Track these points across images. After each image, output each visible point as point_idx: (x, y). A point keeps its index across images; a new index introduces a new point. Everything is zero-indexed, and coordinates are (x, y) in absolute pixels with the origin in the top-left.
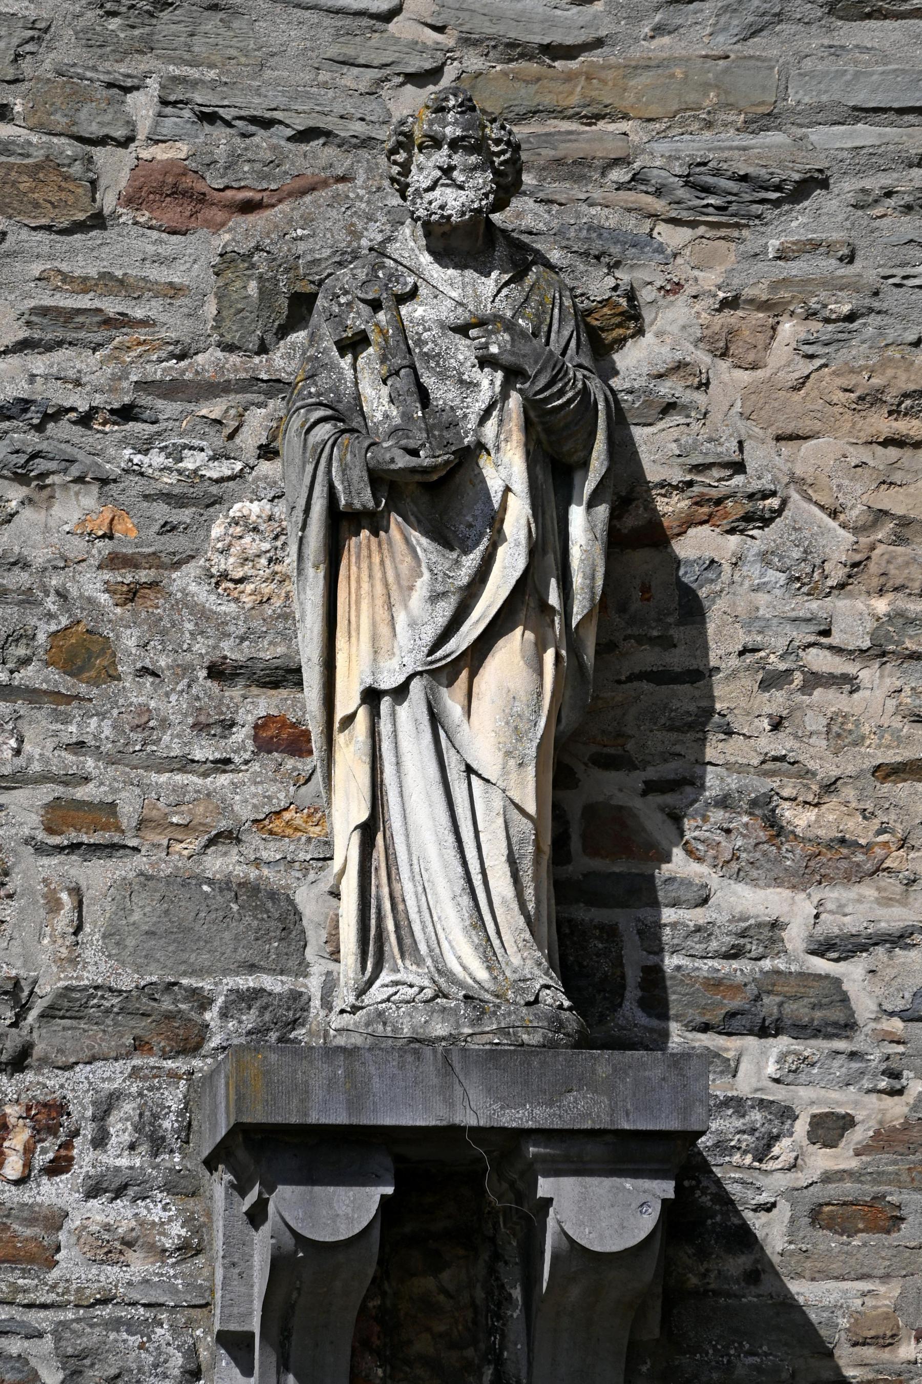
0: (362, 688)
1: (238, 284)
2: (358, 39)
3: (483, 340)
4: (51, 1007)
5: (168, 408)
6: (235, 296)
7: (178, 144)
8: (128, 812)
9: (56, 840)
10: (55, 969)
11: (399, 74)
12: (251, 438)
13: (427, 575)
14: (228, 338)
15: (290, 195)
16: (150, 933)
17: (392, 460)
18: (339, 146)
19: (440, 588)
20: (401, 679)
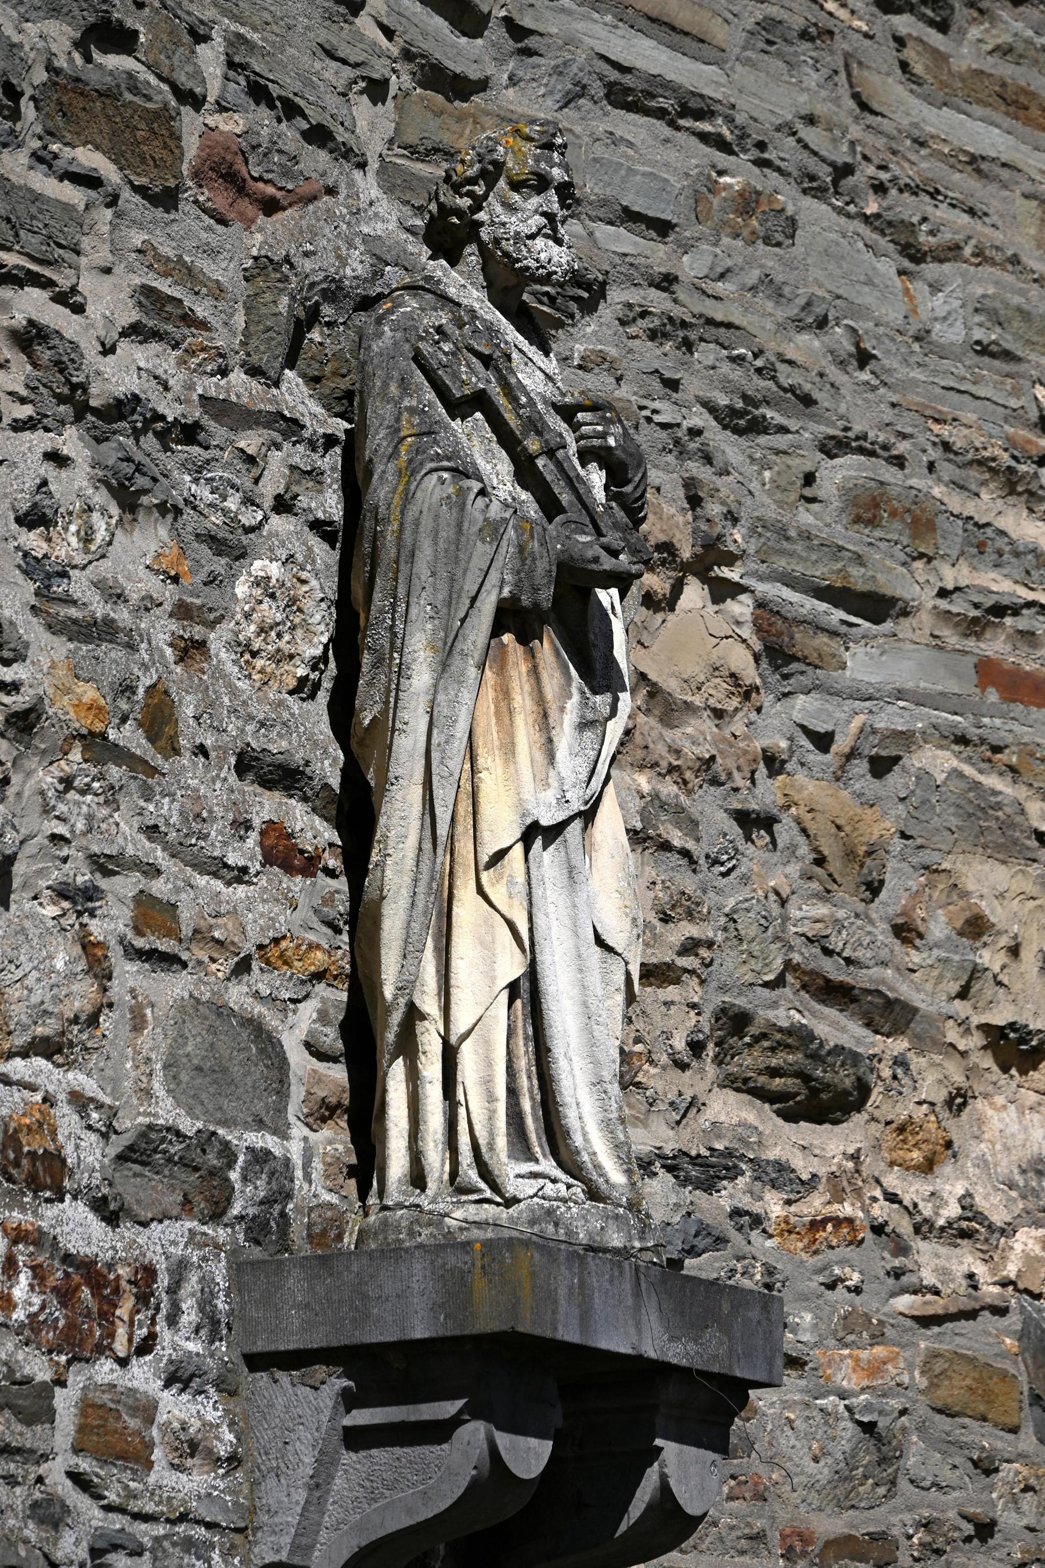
0: (529, 821)
1: (268, 297)
2: (335, 27)
3: (600, 428)
4: (131, 1148)
5: (217, 432)
6: (264, 310)
7: (236, 116)
8: (187, 917)
9: (140, 943)
10: (135, 1101)
11: (363, 78)
12: (273, 483)
13: (576, 697)
14: (255, 359)
15: (300, 200)
16: (199, 1069)
17: (596, 560)
18: (331, 152)
19: (590, 716)
20: (561, 817)
